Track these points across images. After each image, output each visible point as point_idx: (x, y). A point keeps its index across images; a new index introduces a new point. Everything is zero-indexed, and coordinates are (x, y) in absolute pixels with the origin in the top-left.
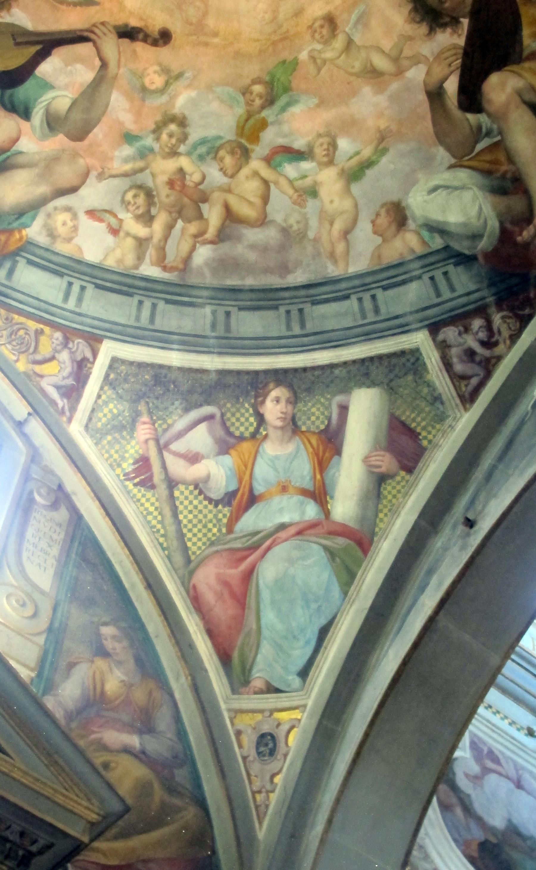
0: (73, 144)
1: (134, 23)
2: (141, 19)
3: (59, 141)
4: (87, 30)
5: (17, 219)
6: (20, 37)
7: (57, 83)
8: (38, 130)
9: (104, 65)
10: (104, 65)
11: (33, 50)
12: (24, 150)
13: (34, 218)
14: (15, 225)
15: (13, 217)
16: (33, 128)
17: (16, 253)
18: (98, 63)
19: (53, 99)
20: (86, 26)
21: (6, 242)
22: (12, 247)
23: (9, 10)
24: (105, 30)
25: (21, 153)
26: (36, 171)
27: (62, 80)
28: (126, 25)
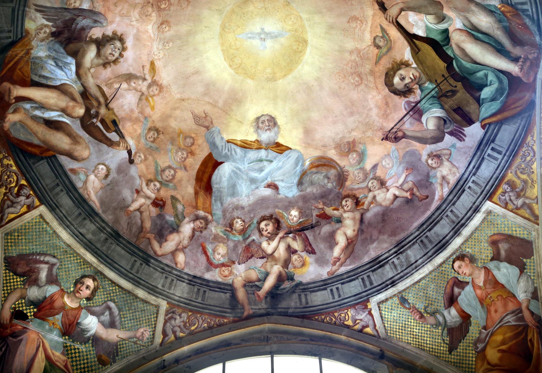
0: (444, 5)
1: (377, 7)
2: (373, 4)
3: (446, 11)
4: (394, 24)
5: (495, 12)
6: (415, 51)
7: (424, 25)
8: (449, 23)
9: (402, 10)
10: (402, 10)
11: (417, 42)
12: (462, 24)
13: (490, 5)
14: (499, 12)
15: (496, 15)
16: (450, 25)
17: (512, 5)
18: (403, 13)
19: (431, 23)
20: (392, 25)
21: (509, 12)
22: (509, 8)
23: (408, 61)
24: (388, 17)
25: (464, 25)
26: (468, 15)
27: (421, 24)
28: (380, 9)
